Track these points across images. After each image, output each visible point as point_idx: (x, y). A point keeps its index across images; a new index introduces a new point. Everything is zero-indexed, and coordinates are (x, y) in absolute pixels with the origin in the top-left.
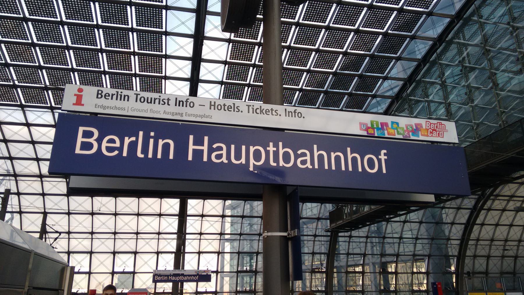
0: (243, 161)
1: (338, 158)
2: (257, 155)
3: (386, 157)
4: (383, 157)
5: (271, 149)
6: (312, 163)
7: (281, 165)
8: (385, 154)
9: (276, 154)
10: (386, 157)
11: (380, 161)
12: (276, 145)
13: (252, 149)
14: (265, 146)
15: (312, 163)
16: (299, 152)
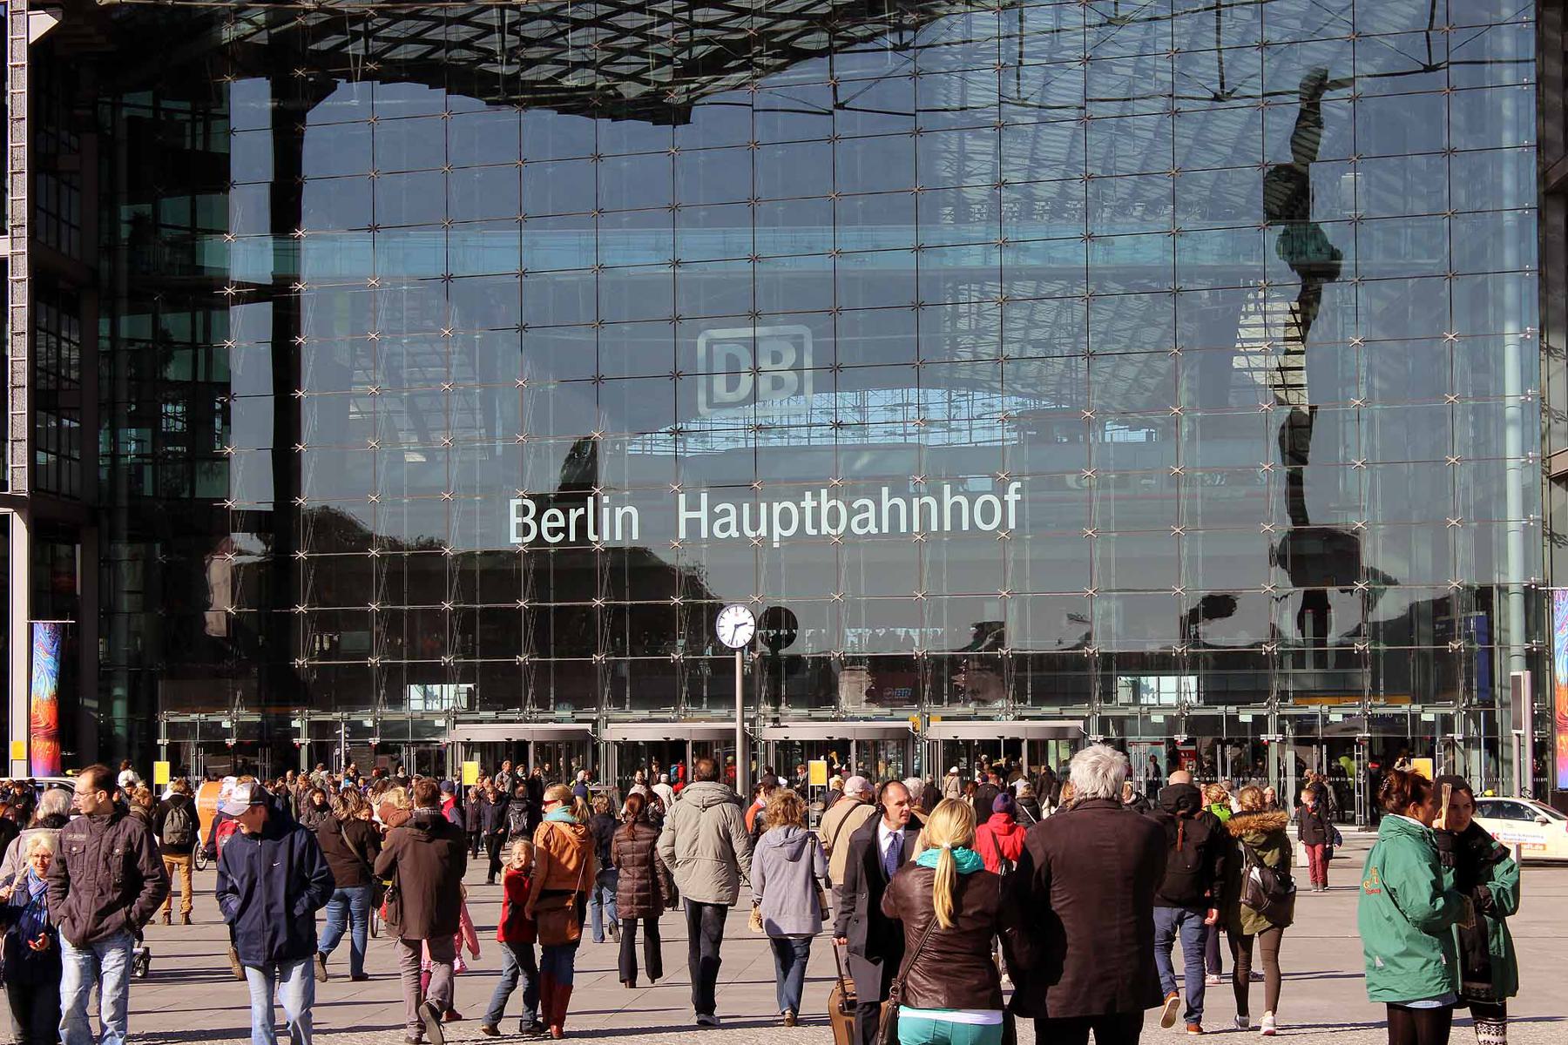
0: (763, 531)
1: (924, 509)
2: (786, 522)
3: (1019, 497)
4: (1012, 497)
5: (808, 503)
6: (879, 525)
7: (824, 532)
8: (1017, 491)
9: (816, 511)
10: (1019, 497)
11: (1004, 504)
12: (816, 496)
13: (777, 508)
14: (798, 499)
15: (879, 525)
16: (855, 505)
